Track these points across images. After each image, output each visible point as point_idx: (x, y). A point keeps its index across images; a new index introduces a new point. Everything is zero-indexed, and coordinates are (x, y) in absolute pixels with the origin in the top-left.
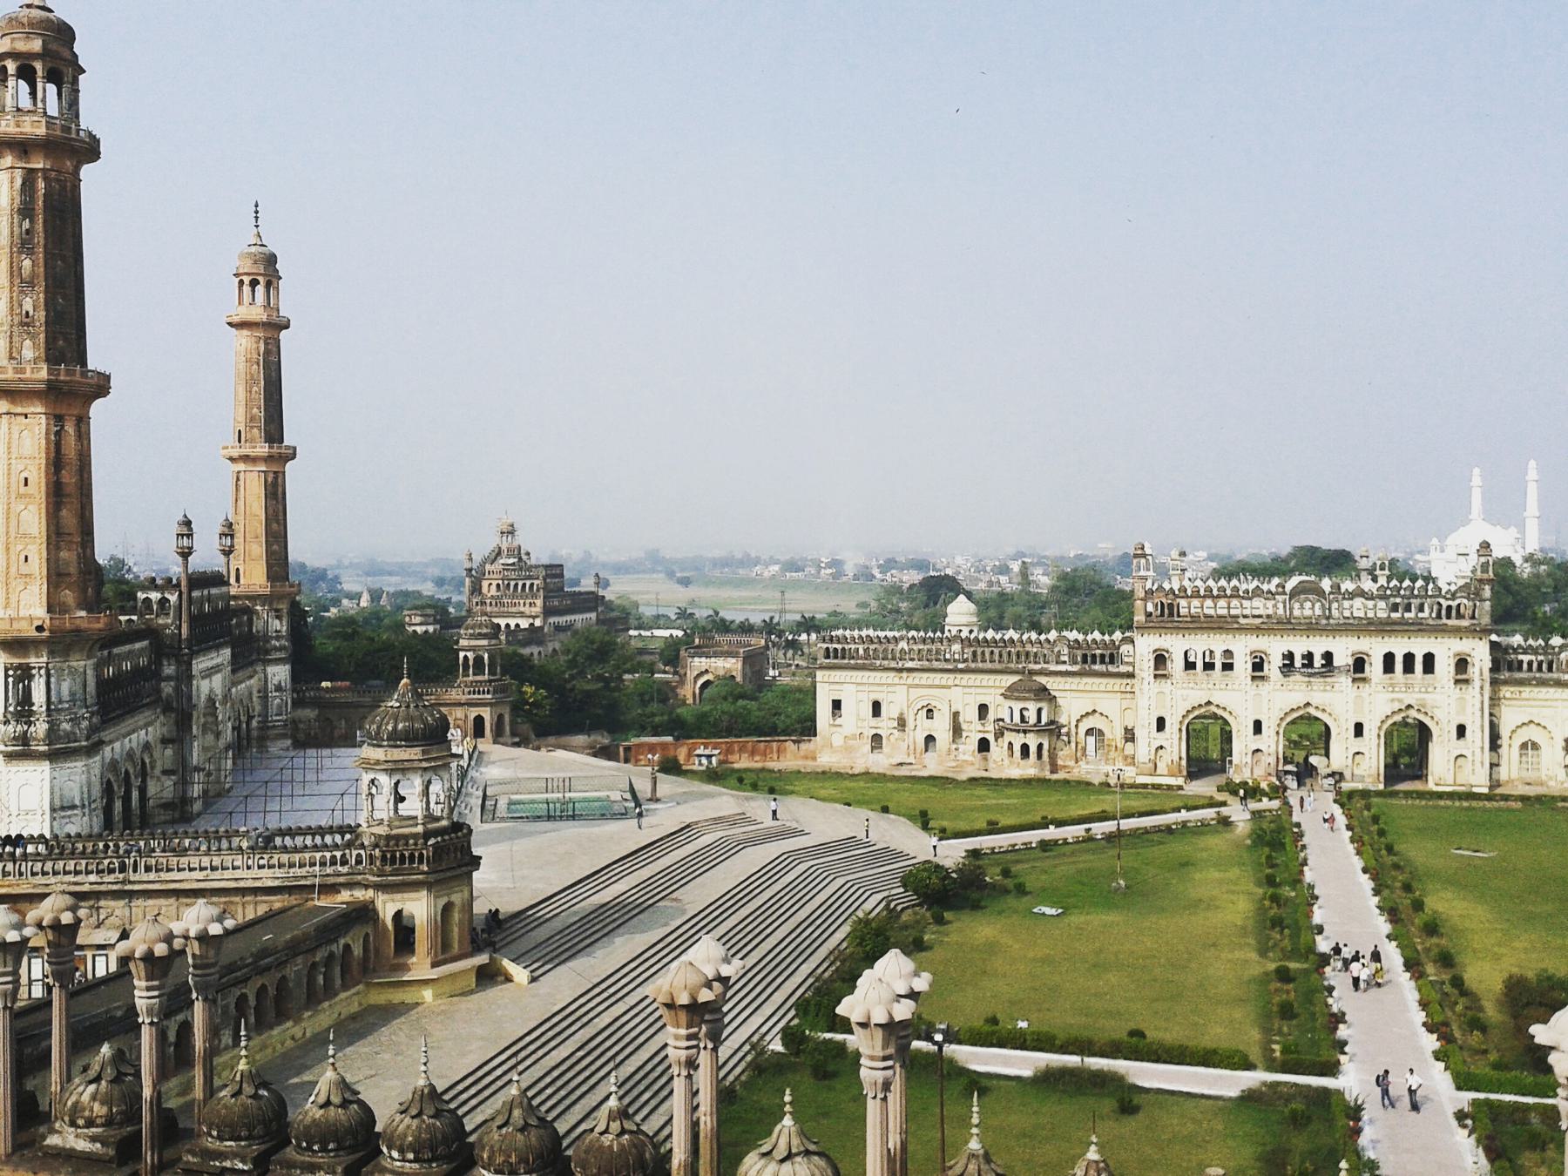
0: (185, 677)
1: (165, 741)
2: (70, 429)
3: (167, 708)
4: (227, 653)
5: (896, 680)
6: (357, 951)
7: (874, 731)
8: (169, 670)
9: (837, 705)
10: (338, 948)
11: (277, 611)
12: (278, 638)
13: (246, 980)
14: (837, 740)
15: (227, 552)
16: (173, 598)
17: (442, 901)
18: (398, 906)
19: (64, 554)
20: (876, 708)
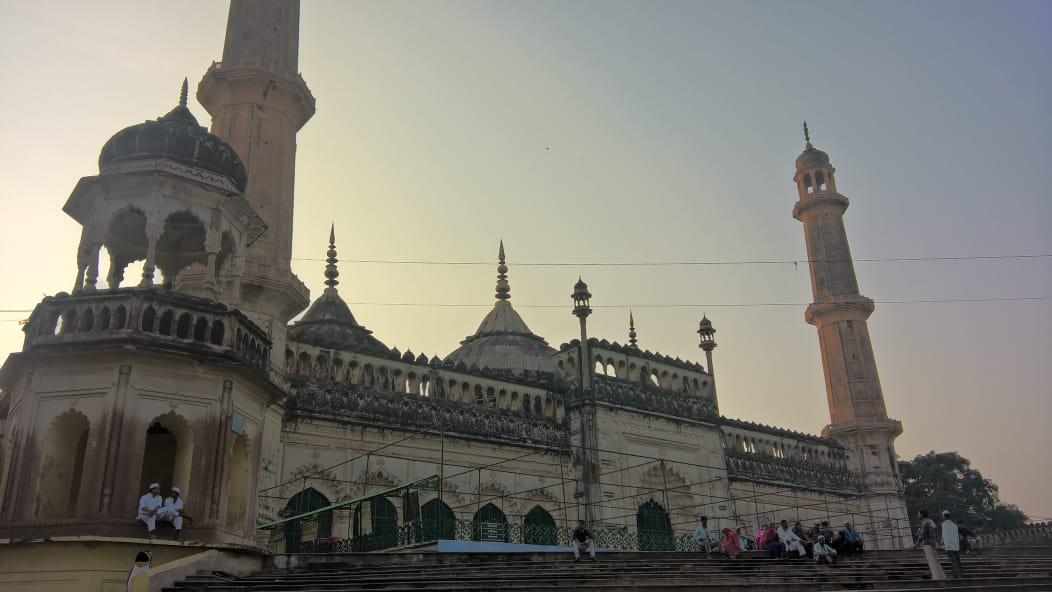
0: (590, 428)
4: (709, 442)
8: (575, 425)
11: (872, 447)
15: (708, 347)
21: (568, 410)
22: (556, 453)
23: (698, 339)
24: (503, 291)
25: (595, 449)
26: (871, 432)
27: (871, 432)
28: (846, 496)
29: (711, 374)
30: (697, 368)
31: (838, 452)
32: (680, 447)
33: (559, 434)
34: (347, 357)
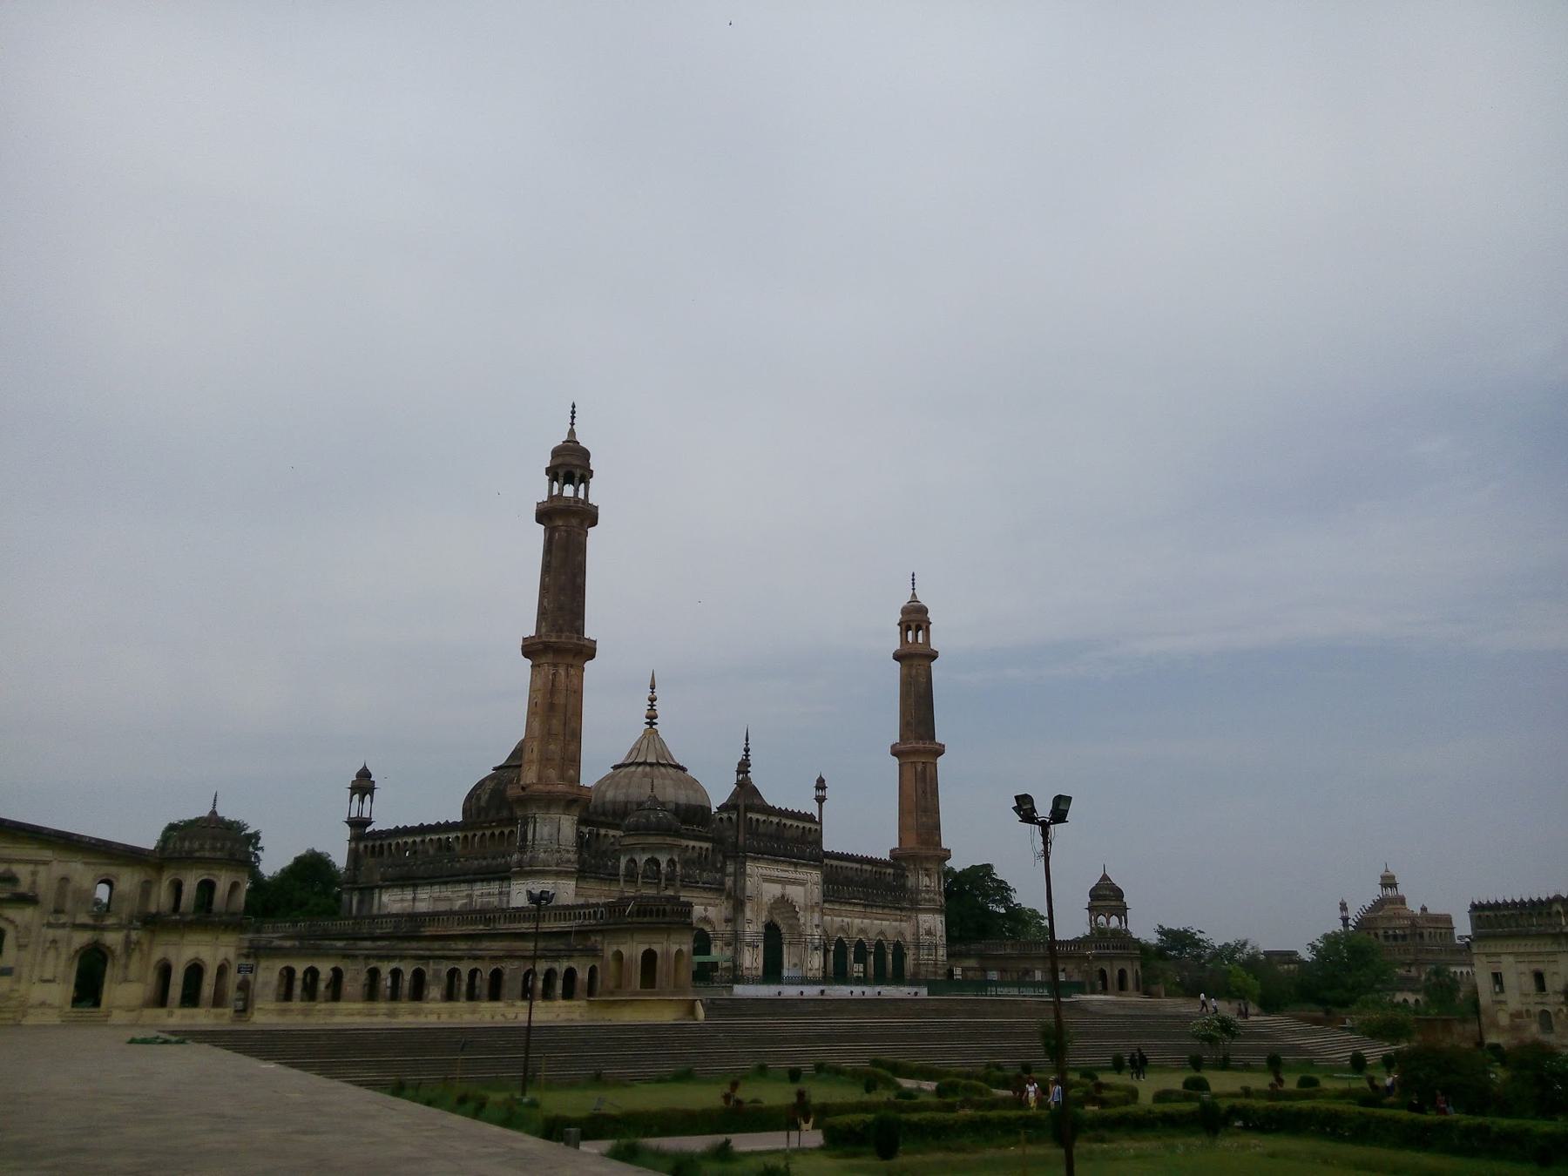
0: (740, 874)
1: (727, 921)
2: (562, 671)
3: (729, 897)
4: (815, 876)
5: (1555, 948)
6: (582, 976)
7: (1541, 1008)
8: (730, 869)
9: (1497, 978)
10: (561, 967)
12: (928, 892)
13: (459, 958)
14: (1504, 1019)
15: (820, 800)
16: (734, 817)
17: (646, 947)
18: (615, 948)
19: (552, 747)
20: (1539, 977)
21: (725, 857)
22: (717, 890)
23: (813, 793)
24: (651, 719)
25: (743, 889)
26: (927, 859)
27: (927, 859)
28: (901, 909)
29: (820, 823)
30: (809, 818)
31: (901, 876)
32: (794, 882)
33: (718, 876)
34: (603, 832)
